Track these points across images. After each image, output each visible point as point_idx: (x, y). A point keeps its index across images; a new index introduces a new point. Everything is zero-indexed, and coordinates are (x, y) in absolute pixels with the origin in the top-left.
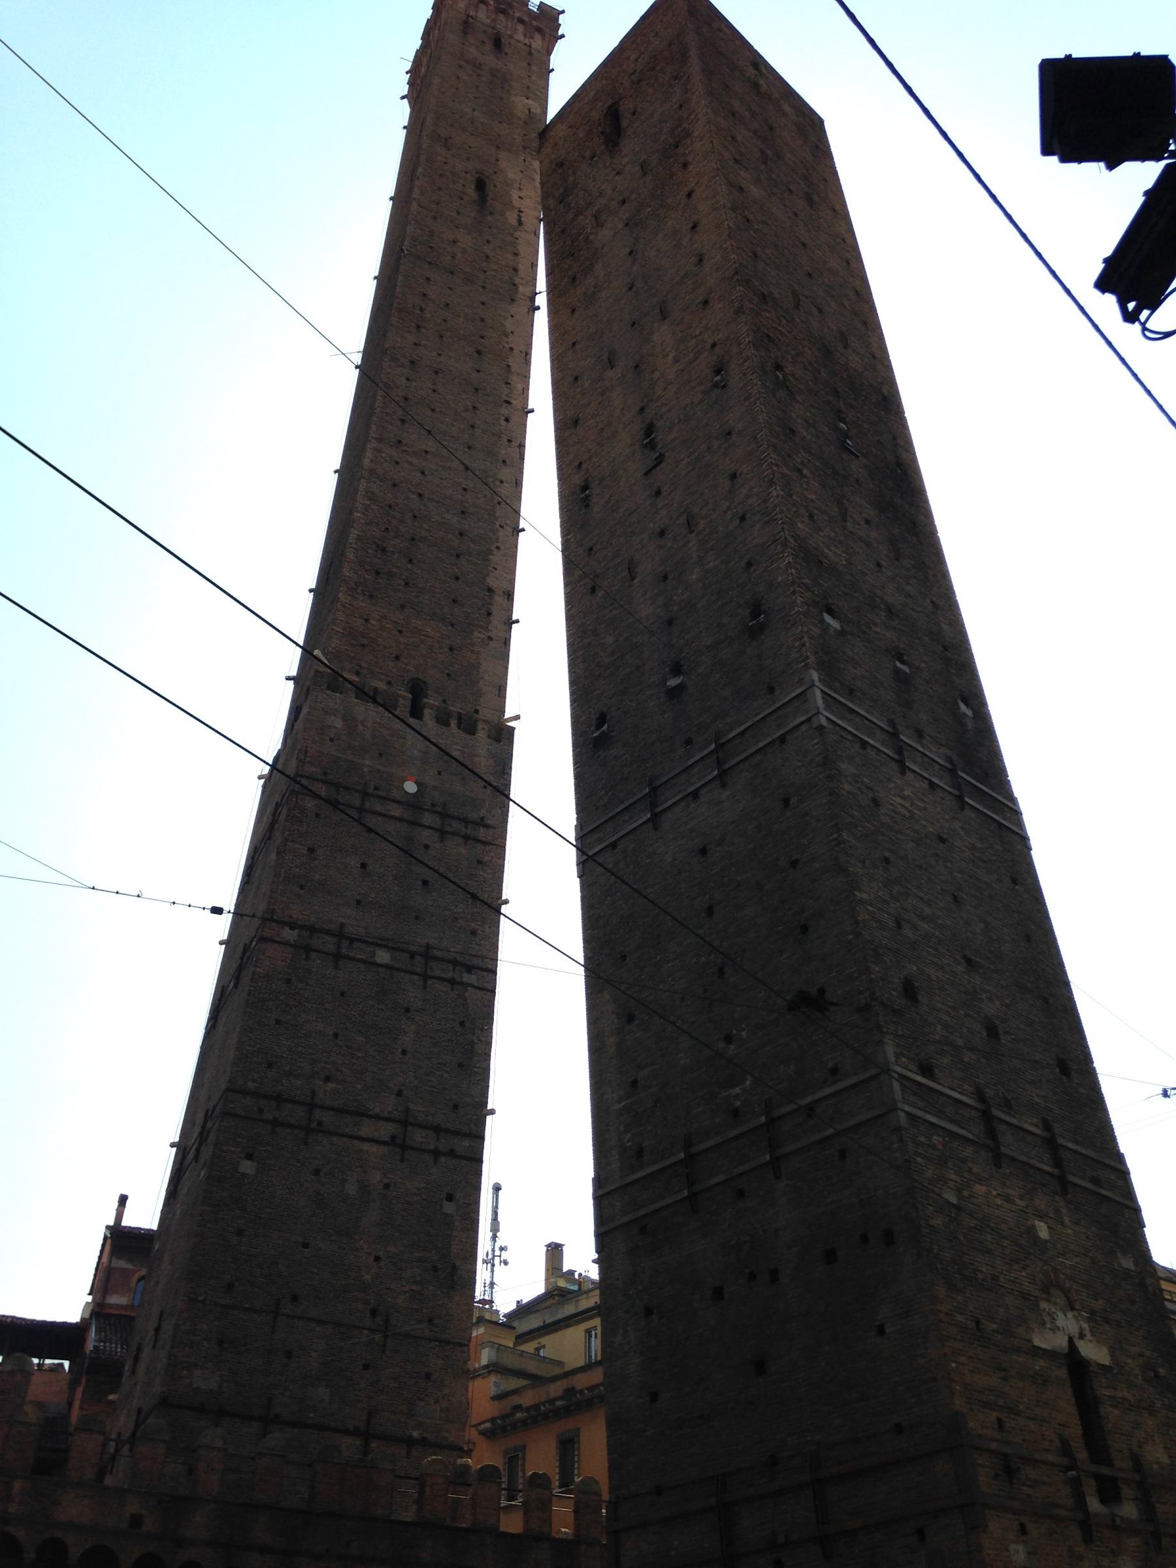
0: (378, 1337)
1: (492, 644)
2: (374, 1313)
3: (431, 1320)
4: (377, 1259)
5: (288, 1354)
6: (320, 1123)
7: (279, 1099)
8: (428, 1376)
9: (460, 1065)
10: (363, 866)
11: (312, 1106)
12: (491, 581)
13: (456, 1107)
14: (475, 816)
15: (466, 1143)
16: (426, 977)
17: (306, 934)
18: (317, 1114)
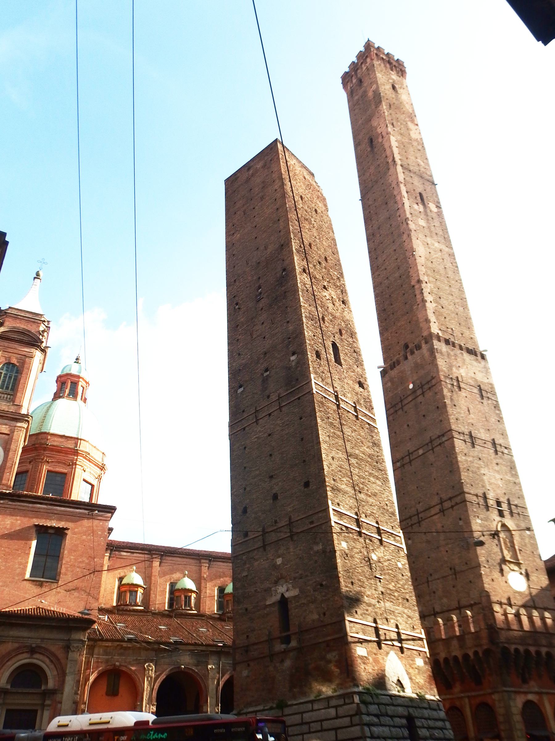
0: (454, 576)
1: (419, 306)
2: (451, 569)
3: (466, 564)
4: (447, 551)
5: (434, 592)
6: (422, 518)
7: (410, 517)
8: (470, 582)
9: (451, 471)
10: (408, 425)
11: (418, 514)
12: (413, 283)
13: (453, 487)
14: (429, 378)
15: (459, 497)
16: (433, 449)
17: (401, 461)
18: (420, 516)
